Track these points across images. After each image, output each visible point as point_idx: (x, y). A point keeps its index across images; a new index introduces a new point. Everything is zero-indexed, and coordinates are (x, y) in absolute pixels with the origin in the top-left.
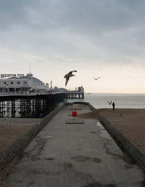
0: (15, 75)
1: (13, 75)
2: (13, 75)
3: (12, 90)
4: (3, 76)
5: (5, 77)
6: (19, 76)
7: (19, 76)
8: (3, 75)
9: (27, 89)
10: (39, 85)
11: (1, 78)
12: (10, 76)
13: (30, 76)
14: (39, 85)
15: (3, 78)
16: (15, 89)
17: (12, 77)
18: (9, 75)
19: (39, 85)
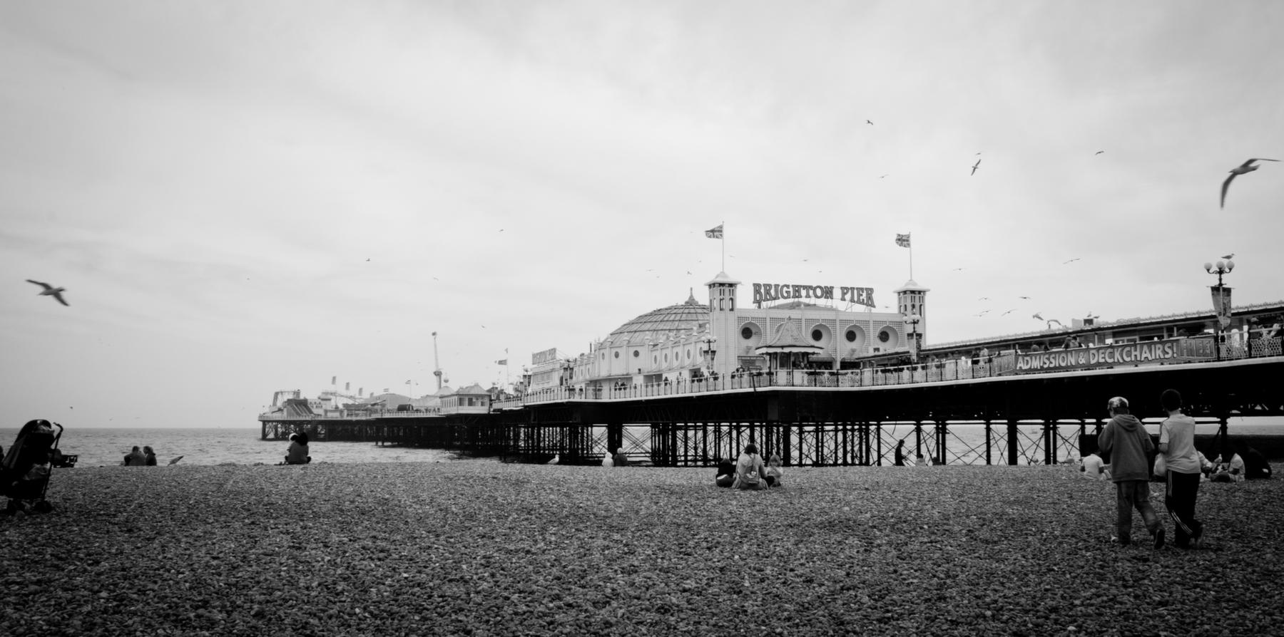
0: (828, 292)
1: (819, 292)
4: (768, 292)
6: (848, 297)
7: (848, 297)
8: (767, 287)
12: (803, 293)
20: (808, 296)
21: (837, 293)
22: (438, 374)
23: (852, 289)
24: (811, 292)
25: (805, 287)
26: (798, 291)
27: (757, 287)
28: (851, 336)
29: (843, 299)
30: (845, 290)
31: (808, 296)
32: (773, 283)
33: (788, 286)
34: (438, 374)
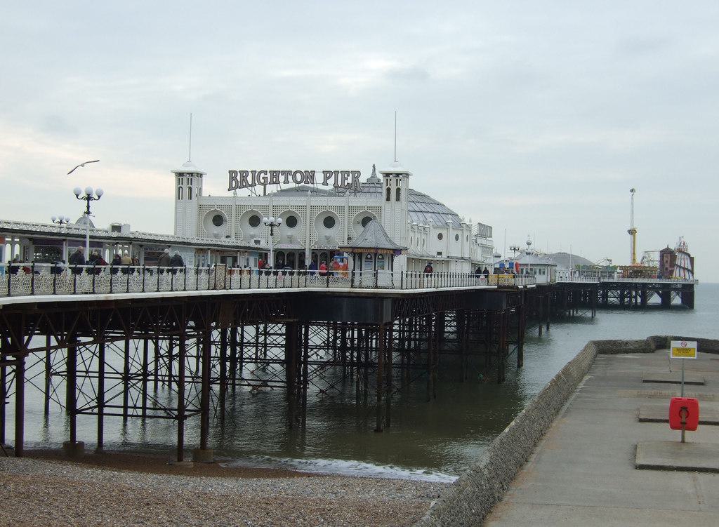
0: (309, 176)
1: (299, 177)
2: (299, 177)
3: (288, 260)
4: (244, 178)
5: (253, 185)
6: (331, 181)
7: (331, 181)
8: (244, 174)
9: (379, 256)
10: (444, 232)
11: (231, 194)
12: (282, 178)
13: (393, 185)
14: (440, 237)
15: (243, 193)
16: (308, 254)
17: (292, 185)
18: (275, 174)
19: (440, 237)
20: (286, 182)
21: (319, 178)
22: (632, 232)
23: (337, 172)
24: (290, 178)
25: (283, 173)
26: (277, 177)
27: (233, 174)
28: (329, 222)
29: (325, 183)
30: (327, 175)
31: (286, 182)
32: (249, 170)
33: (265, 172)
34: (632, 232)
